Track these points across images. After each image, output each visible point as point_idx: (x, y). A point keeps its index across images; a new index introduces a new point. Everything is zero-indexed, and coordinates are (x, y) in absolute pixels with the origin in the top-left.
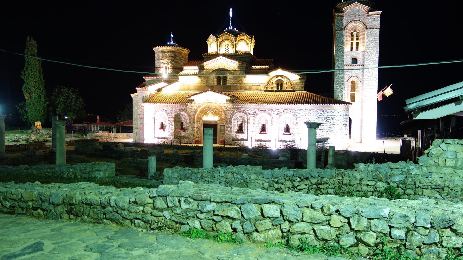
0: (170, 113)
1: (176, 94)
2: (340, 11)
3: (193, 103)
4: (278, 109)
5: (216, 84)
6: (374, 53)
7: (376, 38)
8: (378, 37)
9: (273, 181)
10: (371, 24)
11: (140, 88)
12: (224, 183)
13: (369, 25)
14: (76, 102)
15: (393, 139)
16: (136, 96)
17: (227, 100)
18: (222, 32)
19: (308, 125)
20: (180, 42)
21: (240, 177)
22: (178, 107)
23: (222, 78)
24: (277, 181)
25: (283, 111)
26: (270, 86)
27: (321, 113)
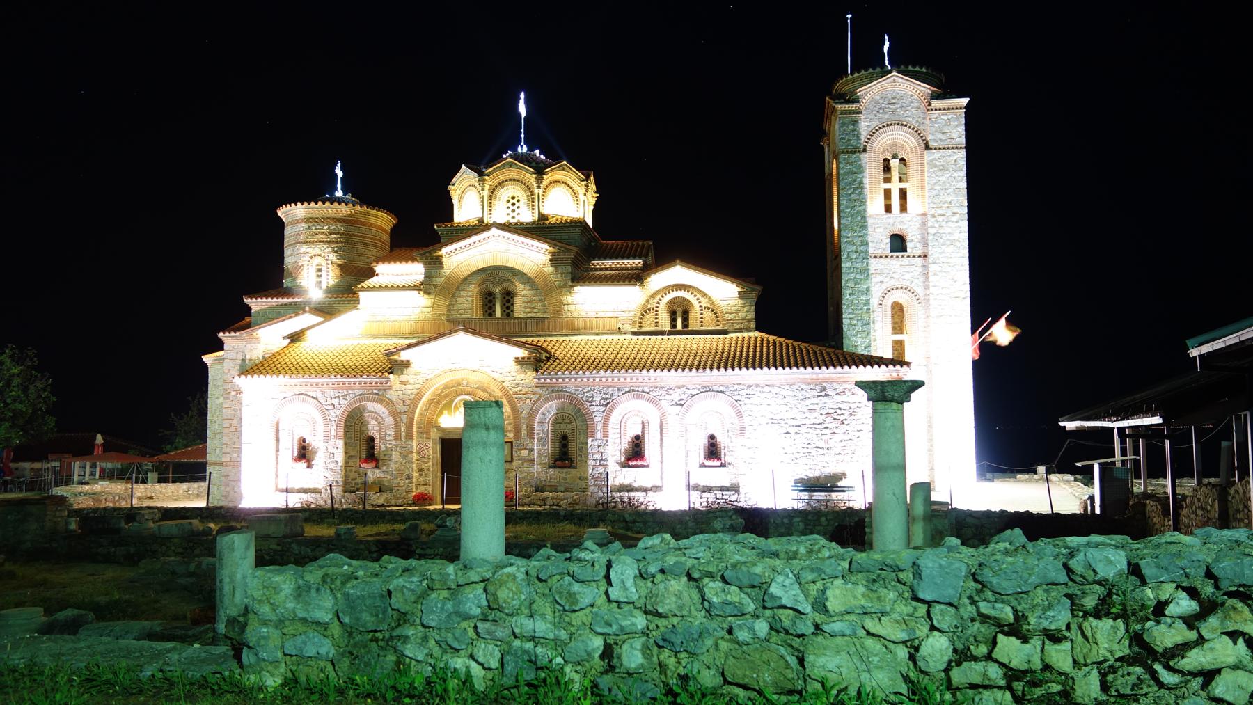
0: (331, 407)
1: (350, 349)
2: (850, 98)
3: (406, 371)
4: (683, 386)
5: (480, 315)
6: (954, 219)
8: (963, 174)
9: (985, 618)
10: (940, 136)
11: (233, 334)
12: (638, 643)
13: (933, 137)
14: (25, 389)
15: (1012, 480)
16: (220, 361)
17: (519, 361)
18: (497, 158)
19: (871, 388)
20: (361, 191)
21: (746, 600)
22: (356, 388)
23: (498, 296)
24: (1019, 618)
26: (649, 318)
27: (818, 396)
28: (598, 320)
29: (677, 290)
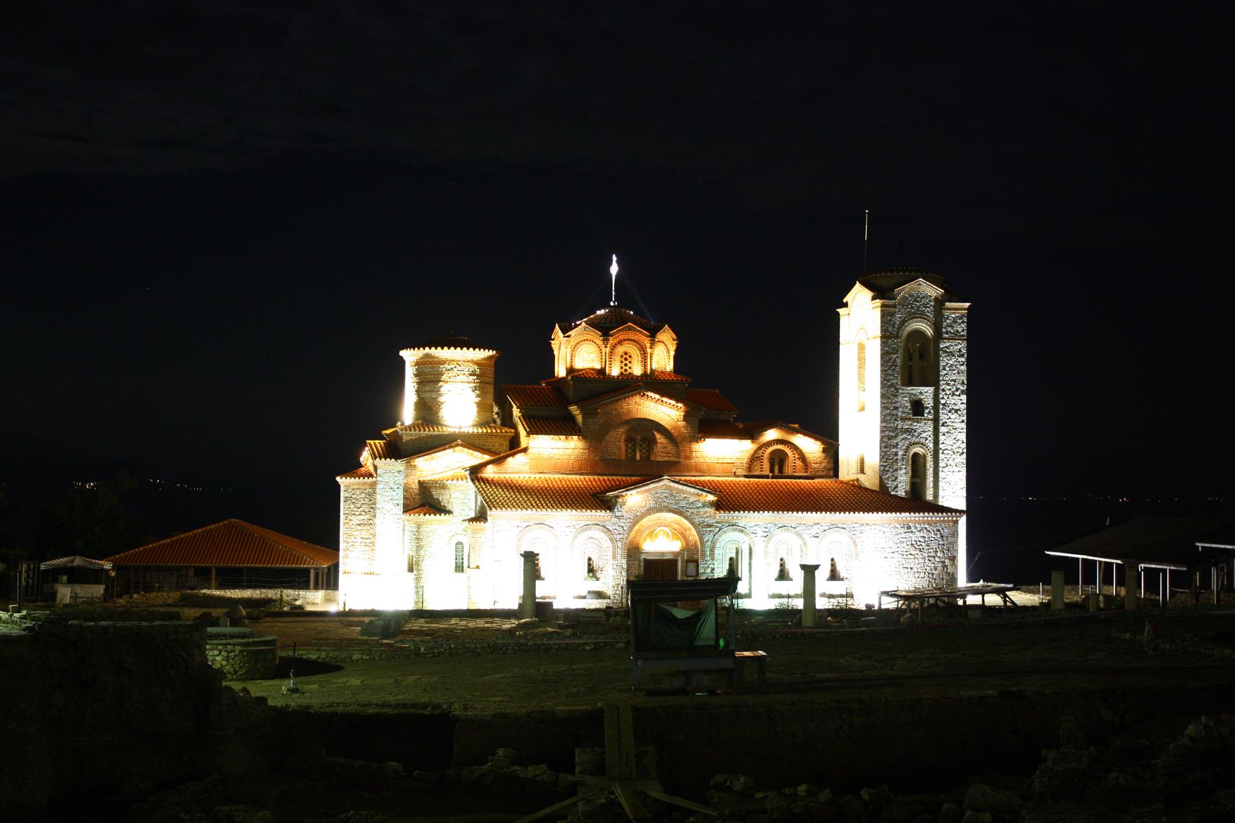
6: (957, 393)
25: (827, 528)
27: (906, 532)
29: (777, 444)
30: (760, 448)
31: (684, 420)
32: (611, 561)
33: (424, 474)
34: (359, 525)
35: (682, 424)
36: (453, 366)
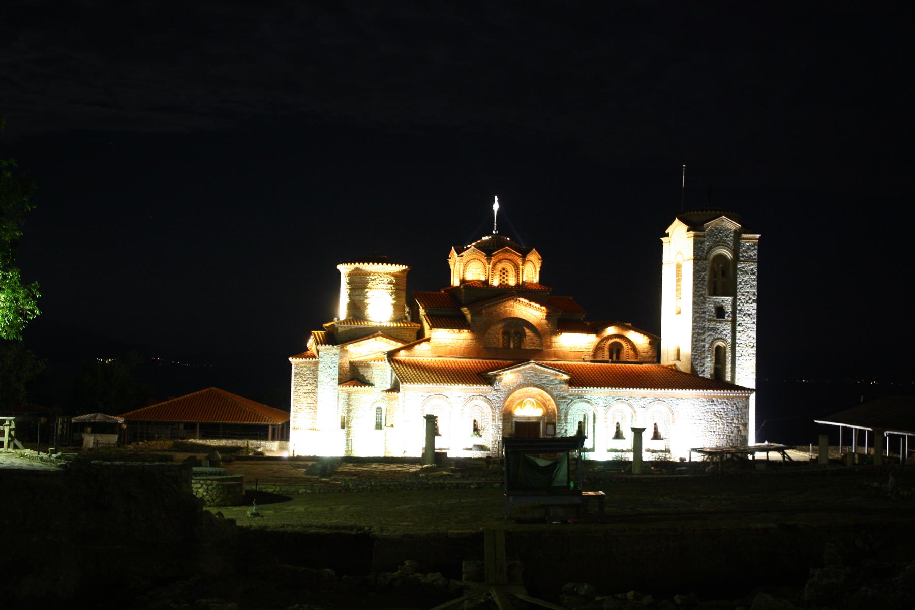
4: (645, 397)
6: (750, 302)
7: (752, 277)
27: (710, 405)
28: (572, 353)
29: (615, 338)
30: (602, 340)
31: (546, 319)
32: (491, 423)
33: (354, 356)
34: (305, 393)
35: (544, 322)
36: (376, 277)
